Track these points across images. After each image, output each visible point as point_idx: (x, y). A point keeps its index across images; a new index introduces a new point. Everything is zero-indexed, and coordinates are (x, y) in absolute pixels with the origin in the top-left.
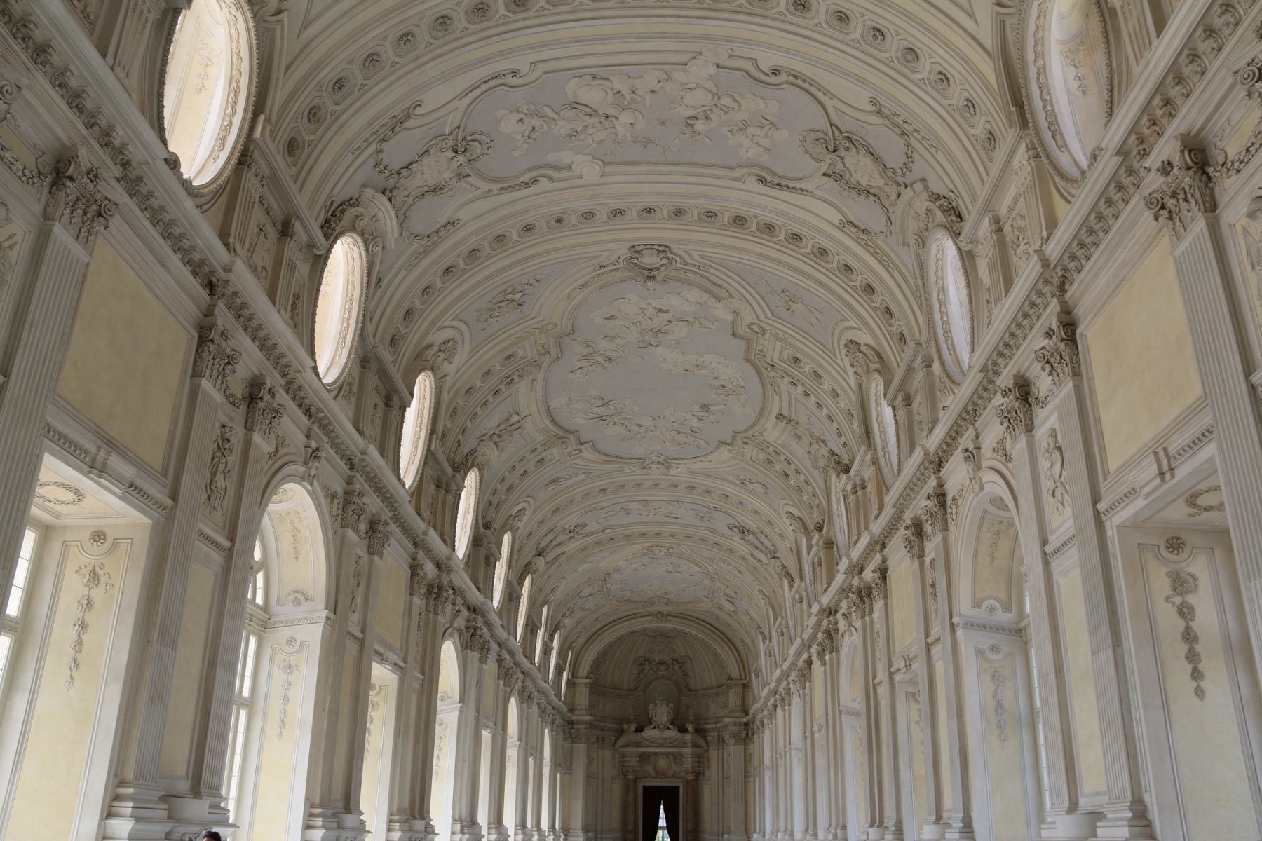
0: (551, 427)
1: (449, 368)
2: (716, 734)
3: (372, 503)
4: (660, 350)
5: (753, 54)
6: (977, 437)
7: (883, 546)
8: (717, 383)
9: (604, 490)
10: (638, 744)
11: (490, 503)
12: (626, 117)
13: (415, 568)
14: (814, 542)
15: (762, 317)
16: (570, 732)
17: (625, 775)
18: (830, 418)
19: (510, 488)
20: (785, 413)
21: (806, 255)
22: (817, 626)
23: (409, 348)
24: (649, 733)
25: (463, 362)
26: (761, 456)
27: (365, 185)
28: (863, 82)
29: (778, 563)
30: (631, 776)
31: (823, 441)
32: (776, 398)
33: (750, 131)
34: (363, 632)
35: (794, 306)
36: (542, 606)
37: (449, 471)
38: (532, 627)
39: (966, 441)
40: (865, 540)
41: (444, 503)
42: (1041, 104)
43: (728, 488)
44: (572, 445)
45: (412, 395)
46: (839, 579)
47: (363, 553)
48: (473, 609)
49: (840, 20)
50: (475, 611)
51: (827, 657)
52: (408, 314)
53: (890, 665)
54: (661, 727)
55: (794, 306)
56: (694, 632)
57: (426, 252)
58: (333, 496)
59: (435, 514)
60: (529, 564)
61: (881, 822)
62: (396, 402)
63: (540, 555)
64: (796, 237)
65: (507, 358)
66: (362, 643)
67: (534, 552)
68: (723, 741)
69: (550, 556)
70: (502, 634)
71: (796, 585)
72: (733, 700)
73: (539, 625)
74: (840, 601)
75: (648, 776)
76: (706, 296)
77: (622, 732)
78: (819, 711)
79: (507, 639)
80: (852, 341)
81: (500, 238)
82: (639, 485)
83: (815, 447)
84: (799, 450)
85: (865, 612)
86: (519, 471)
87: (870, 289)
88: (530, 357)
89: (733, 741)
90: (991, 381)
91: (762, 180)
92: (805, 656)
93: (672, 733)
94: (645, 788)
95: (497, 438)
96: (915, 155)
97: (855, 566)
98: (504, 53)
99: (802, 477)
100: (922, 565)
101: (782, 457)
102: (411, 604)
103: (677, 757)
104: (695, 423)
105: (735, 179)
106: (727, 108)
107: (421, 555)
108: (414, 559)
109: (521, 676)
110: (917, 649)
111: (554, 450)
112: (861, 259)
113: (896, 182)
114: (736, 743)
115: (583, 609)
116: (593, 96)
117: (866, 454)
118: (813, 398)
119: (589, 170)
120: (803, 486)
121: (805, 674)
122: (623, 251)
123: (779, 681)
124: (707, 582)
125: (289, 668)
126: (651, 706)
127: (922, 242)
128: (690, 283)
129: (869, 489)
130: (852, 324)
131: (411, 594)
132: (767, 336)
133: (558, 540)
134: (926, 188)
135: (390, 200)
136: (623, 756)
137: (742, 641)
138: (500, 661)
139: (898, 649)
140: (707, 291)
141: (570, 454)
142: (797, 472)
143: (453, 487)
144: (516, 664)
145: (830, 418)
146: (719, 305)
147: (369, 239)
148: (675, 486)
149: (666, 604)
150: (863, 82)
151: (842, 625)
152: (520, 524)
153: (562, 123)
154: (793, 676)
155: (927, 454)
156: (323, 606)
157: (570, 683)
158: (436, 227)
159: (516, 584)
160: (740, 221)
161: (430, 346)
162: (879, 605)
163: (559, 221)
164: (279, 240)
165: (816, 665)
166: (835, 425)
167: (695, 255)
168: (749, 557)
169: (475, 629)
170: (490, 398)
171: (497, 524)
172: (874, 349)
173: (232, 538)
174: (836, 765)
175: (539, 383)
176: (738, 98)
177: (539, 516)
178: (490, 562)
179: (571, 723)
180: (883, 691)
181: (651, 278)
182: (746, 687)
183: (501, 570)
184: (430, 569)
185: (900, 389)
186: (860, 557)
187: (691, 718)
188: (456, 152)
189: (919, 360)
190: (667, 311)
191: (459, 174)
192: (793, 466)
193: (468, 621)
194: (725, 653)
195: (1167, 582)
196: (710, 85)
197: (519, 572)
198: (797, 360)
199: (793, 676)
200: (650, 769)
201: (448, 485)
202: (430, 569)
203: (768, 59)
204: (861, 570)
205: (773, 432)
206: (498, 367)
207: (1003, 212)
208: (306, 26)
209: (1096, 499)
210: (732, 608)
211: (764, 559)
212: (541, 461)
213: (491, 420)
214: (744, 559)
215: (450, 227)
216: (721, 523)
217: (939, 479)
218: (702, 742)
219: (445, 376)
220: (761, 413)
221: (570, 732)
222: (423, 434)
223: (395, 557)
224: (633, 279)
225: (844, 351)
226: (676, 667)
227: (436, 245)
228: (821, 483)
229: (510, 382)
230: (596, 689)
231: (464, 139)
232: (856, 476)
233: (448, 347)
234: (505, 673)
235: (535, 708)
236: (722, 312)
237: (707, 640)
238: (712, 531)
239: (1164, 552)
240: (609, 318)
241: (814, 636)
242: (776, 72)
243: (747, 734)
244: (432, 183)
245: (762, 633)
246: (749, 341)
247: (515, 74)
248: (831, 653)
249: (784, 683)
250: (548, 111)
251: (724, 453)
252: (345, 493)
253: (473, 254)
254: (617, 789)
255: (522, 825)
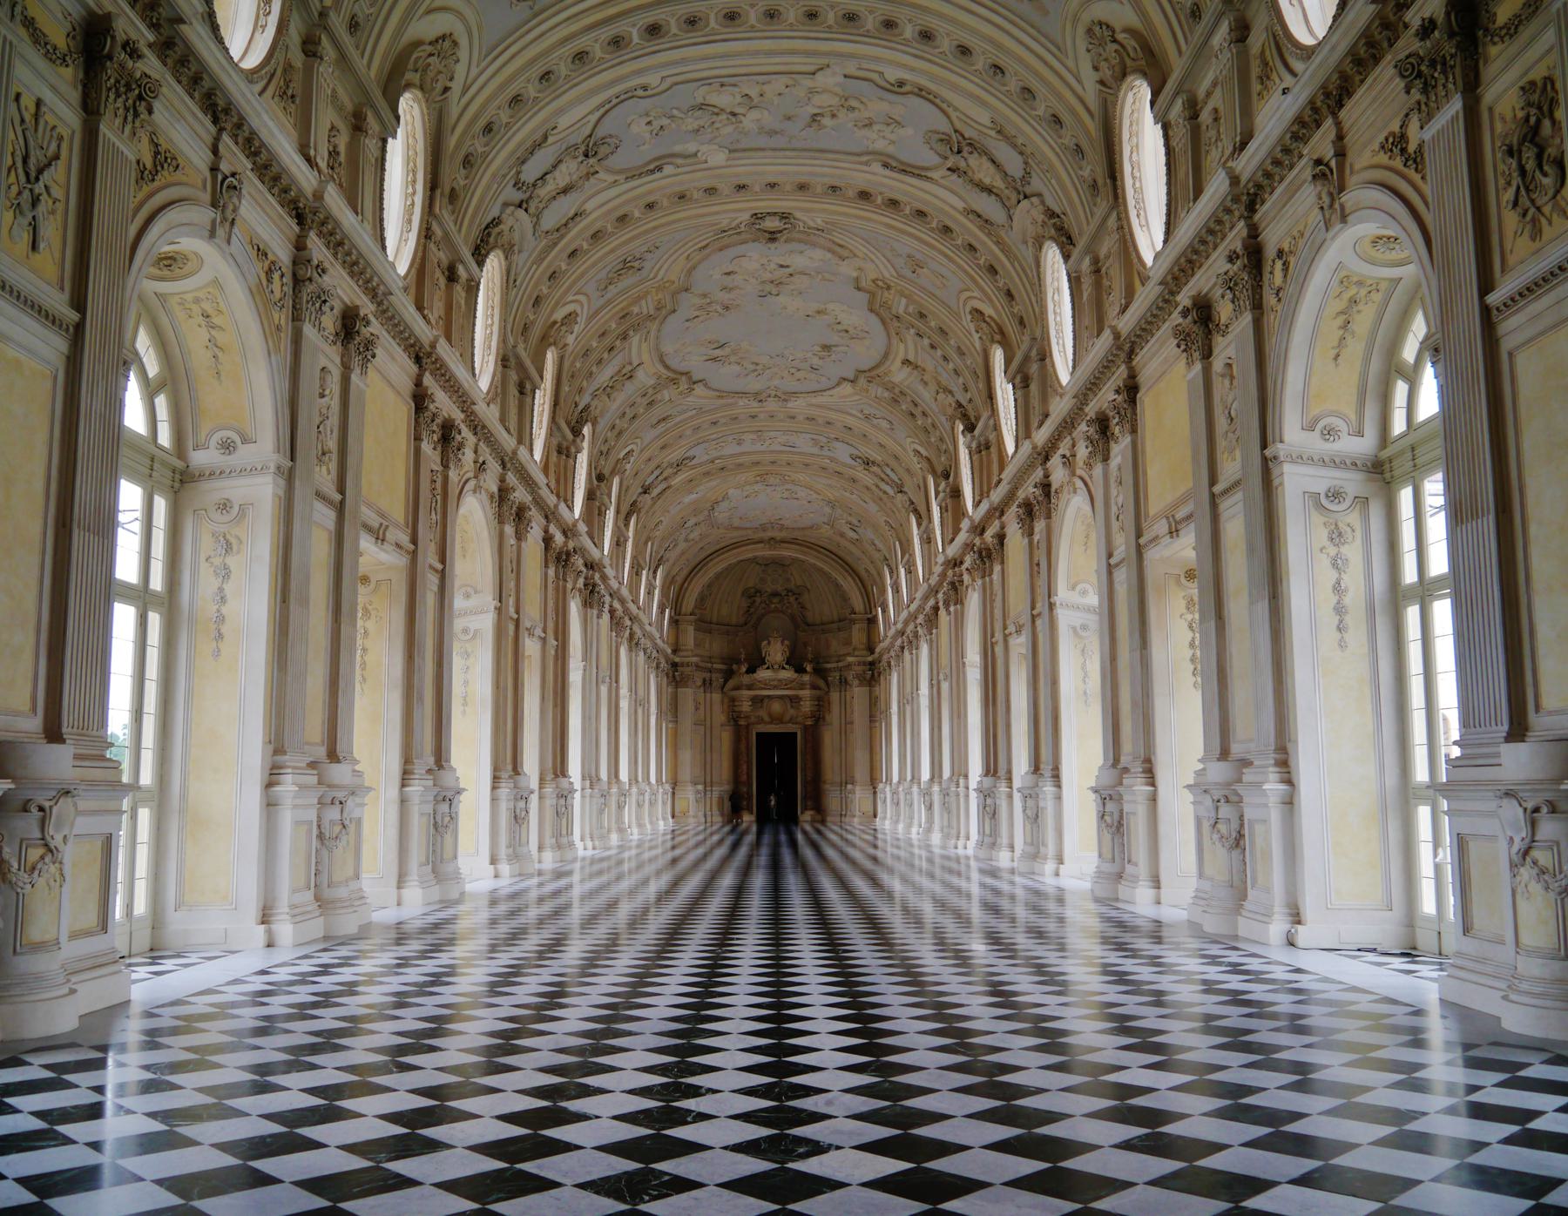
0: (663, 371)
1: (570, 339)
2: (837, 675)
3: (520, 495)
4: (781, 299)
5: (880, 69)
6: (1074, 446)
7: (1002, 513)
8: (840, 327)
9: (715, 423)
10: (750, 687)
11: (602, 453)
12: (754, 115)
13: (547, 540)
14: (941, 488)
15: (887, 275)
16: (674, 676)
17: (736, 721)
18: (956, 372)
19: (620, 433)
20: (911, 358)
21: (932, 230)
22: (943, 575)
23: (536, 332)
24: (763, 674)
25: (583, 326)
26: (886, 394)
27: (506, 205)
28: (984, 104)
29: (906, 498)
30: (742, 722)
31: (950, 392)
32: (902, 346)
33: (876, 127)
34: (517, 612)
35: (919, 270)
36: (646, 543)
37: (570, 436)
38: (636, 570)
39: (1064, 448)
40: (985, 506)
41: (566, 468)
42: (1131, 182)
43: (851, 421)
44: (684, 385)
45: (542, 378)
46: (962, 537)
47: (513, 541)
48: (590, 566)
49: (963, 53)
50: (592, 567)
51: (952, 609)
52: (537, 302)
53: (1005, 628)
54: (776, 667)
55: (919, 270)
56: (813, 561)
57: (555, 244)
58: (492, 497)
59: (558, 482)
60: (635, 502)
61: (996, 771)
62: (528, 386)
63: (645, 493)
64: (921, 214)
65: (624, 317)
66: (517, 623)
67: (640, 490)
68: (846, 682)
69: (655, 492)
70: (614, 584)
71: (924, 523)
72: (858, 635)
73: (642, 562)
74: (963, 554)
75: (761, 721)
76: (829, 255)
77: (729, 674)
78: (944, 661)
79: (619, 589)
80: (977, 311)
81: (623, 219)
82: (753, 417)
83: (941, 396)
84: (926, 395)
85: (986, 573)
86: (629, 415)
87: (992, 270)
88: (645, 311)
89: (856, 682)
90: (1081, 409)
91: (886, 165)
92: (931, 602)
93: (788, 674)
94: (758, 734)
95: (609, 390)
96: (1033, 174)
97: (976, 527)
98: (639, 72)
99: (930, 421)
100: (1031, 543)
101: (909, 399)
102: (546, 574)
103: (795, 701)
104: (816, 361)
105: (861, 163)
106: (854, 109)
107: (553, 529)
108: (546, 531)
109: (628, 623)
110: (1025, 619)
111: (665, 392)
112: (984, 243)
113: (1016, 189)
114: (860, 685)
115: (686, 540)
116: (724, 99)
117: (989, 418)
118: (939, 352)
119: (718, 158)
120: (930, 429)
121: (932, 620)
122: (746, 216)
123: (906, 623)
124: (828, 510)
125: (467, 655)
126: (765, 642)
127: (1039, 245)
128: (814, 245)
129: (992, 449)
130: (975, 294)
131: (546, 566)
132: (892, 292)
133: (665, 475)
134: (1043, 203)
135: (526, 210)
136: (733, 700)
137: (867, 571)
138: (612, 611)
139: (1012, 614)
140: (829, 250)
141: (681, 393)
142: (924, 414)
143: (573, 450)
144: (626, 611)
145: (956, 372)
146: (840, 262)
147: (508, 251)
148: (793, 418)
149: (781, 530)
150: (984, 104)
151: (966, 577)
152: (628, 466)
153: (690, 120)
154: (920, 619)
155: (1034, 447)
156: (491, 598)
157: (674, 622)
158: (563, 221)
159: (621, 525)
160: (864, 195)
161: (555, 323)
162: (997, 568)
163: (682, 197)
164: (447, 286)
165: (942, 612)
166: (961, 380)
167: (819, 221)
168: (874, 488)
169: (594, 585)
170: (606, 355)
171: (606, 472)
172: (997, 324)
173: (443, 561)
174: (959, 717)
175: (652, 334)
176: (864, 100)
177: (646, 455)
178: (602, 513)
179: (675, 665)
180: (999, 649)
181: (773, 240)
182: (872, 621)
183: (610, 515)
184: (559, 538)
185: (1020, 370)
186: (981, 520)
187: (810, 656)
188: (586, 156)
189: (1034, 353)
190: (788, 267)
191: (588, 174)
192: (920, 409)
193: (586, 578)
194: (848, 585)
195: (1183, 603)
196: (838, 90)
197: (625, 517)
198: (922, 316)
199: (920, 619)
200: (763, 713)
201: (568, 449)
202: (559, 538)
203: (893, 74)
204: (983, 531)
205: (899, 375)
206: (614, 326)
207: (1103, 252)
208: (464, 93)
209: (1139, 535)
210: (855, 536)
211: (891, 492)
212: (651, 404)
213: (604, 376)
214: (868, 488)
215: (578, 219)
216: (843, 453)
217: (1046, 470)
218: (822, 683)
219: (565, 345)
220: (886, 355)
221: (674, 676)
222: (547, 407)
223: (535, 534)
224: (754, 241)
225: (969, 317)
226: (792, 599)
227: (562, 237)
228: (948, 428)
229: (625, 338)
230: (704, 625)
231: (595, 144)
232: (980, 435)
233: (571, 318)
234: (616, 624)
235: (642, 653)
236: (847, 269)
237: (826, 568)
238: (832, 459)
239: (1183, 580)
240: (728, 274)
241: (940, 584)
242: (901, 84)
243: (873, 675)
244: (562, 184)
245: (888, 566)
246: (873, 295)
247: (645, 88)
248: (956, 604)
249: (911, 627)
250: (675, 112)
251: (847, 389)
252: (500, 490)
253: (596, 236)
254: (725, 738)
255: (634, 779)
